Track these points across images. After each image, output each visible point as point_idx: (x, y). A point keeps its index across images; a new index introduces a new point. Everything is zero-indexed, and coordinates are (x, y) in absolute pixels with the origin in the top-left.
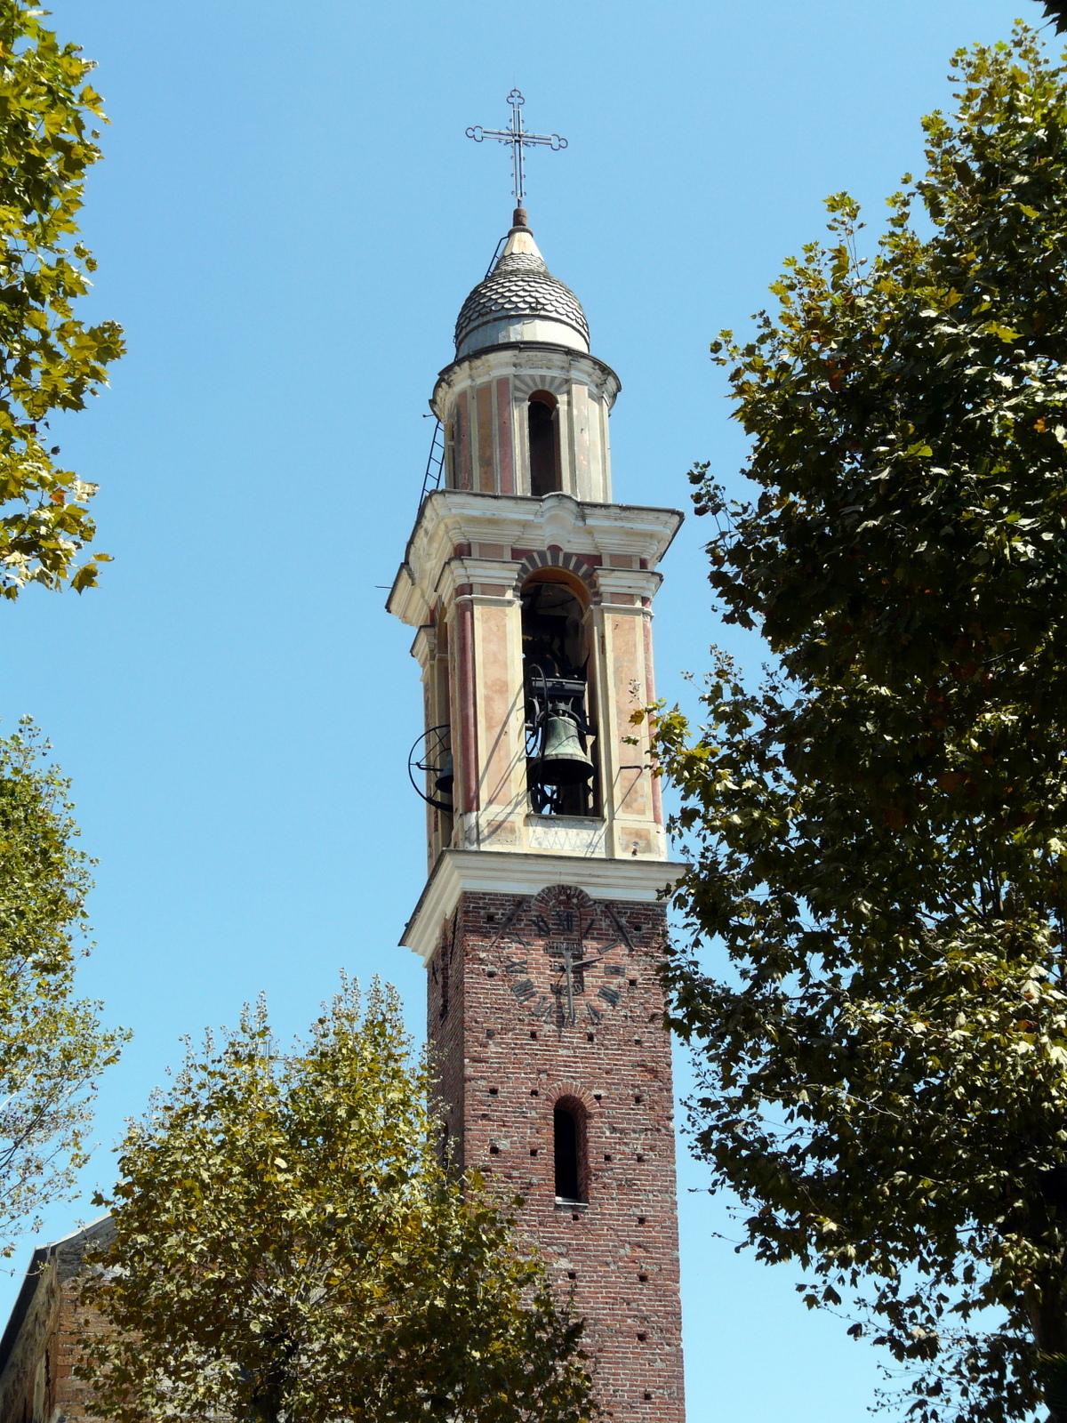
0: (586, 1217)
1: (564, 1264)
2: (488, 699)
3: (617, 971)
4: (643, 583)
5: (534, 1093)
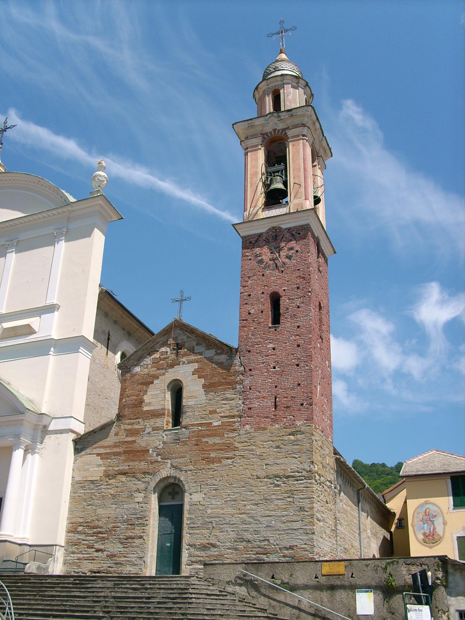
0: (278, 330)
1: (271, 346)
2: (251, 178)
3: (292, 249)
5: (263, 293)
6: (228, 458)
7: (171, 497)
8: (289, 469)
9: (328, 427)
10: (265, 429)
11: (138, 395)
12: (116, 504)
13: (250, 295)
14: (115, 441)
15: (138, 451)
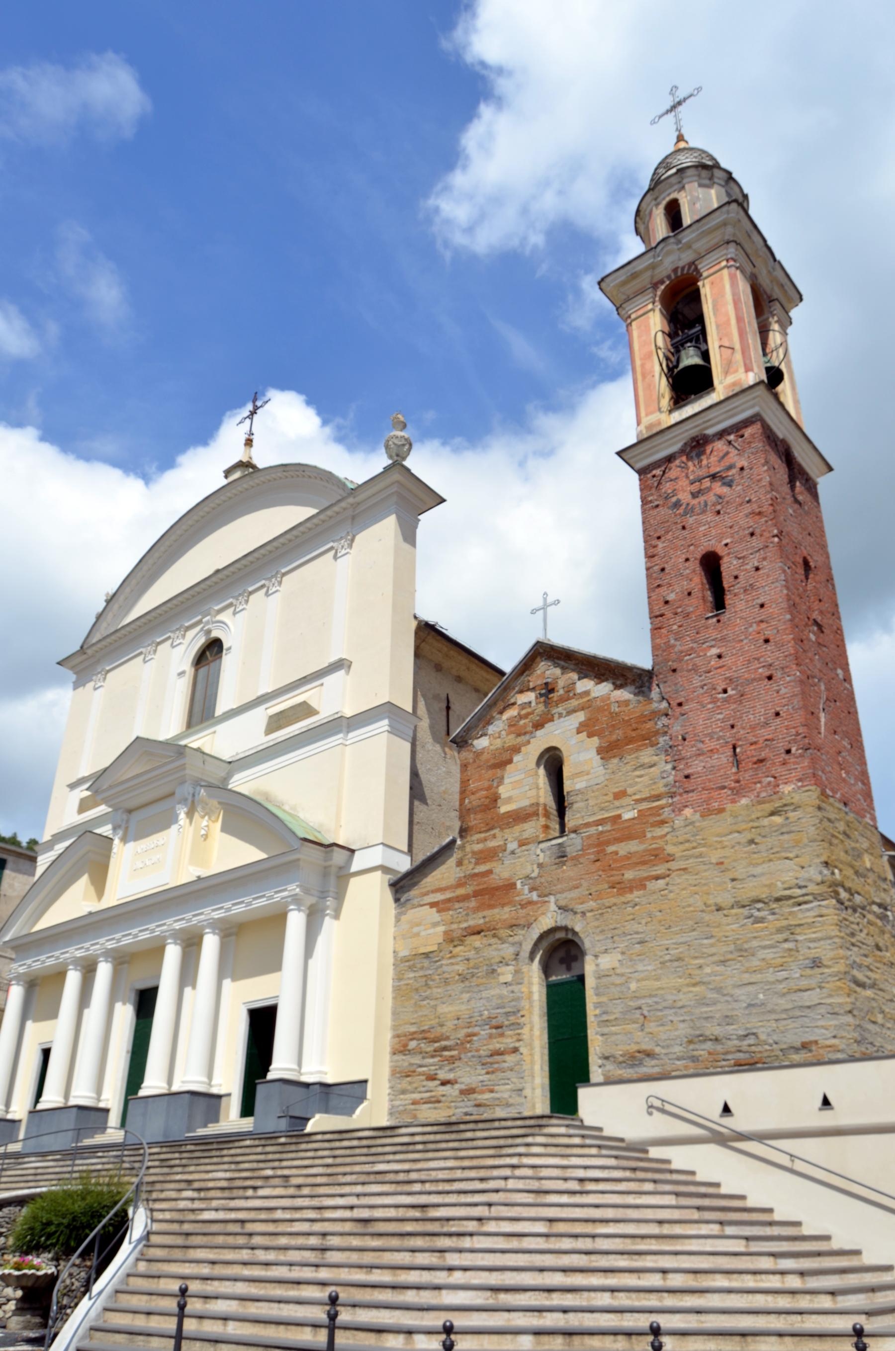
1: (715, 651)
4: (725, 252)
5: (687, 560)
6: (657, 878)
7: (564, 966)
8: (779, 884)
9: (859, 796)
10: (721, 811)
11: (489, 788)
12: (468, 992)
13: (663, 570)
14: (458, 875)
15: (497, 888)
